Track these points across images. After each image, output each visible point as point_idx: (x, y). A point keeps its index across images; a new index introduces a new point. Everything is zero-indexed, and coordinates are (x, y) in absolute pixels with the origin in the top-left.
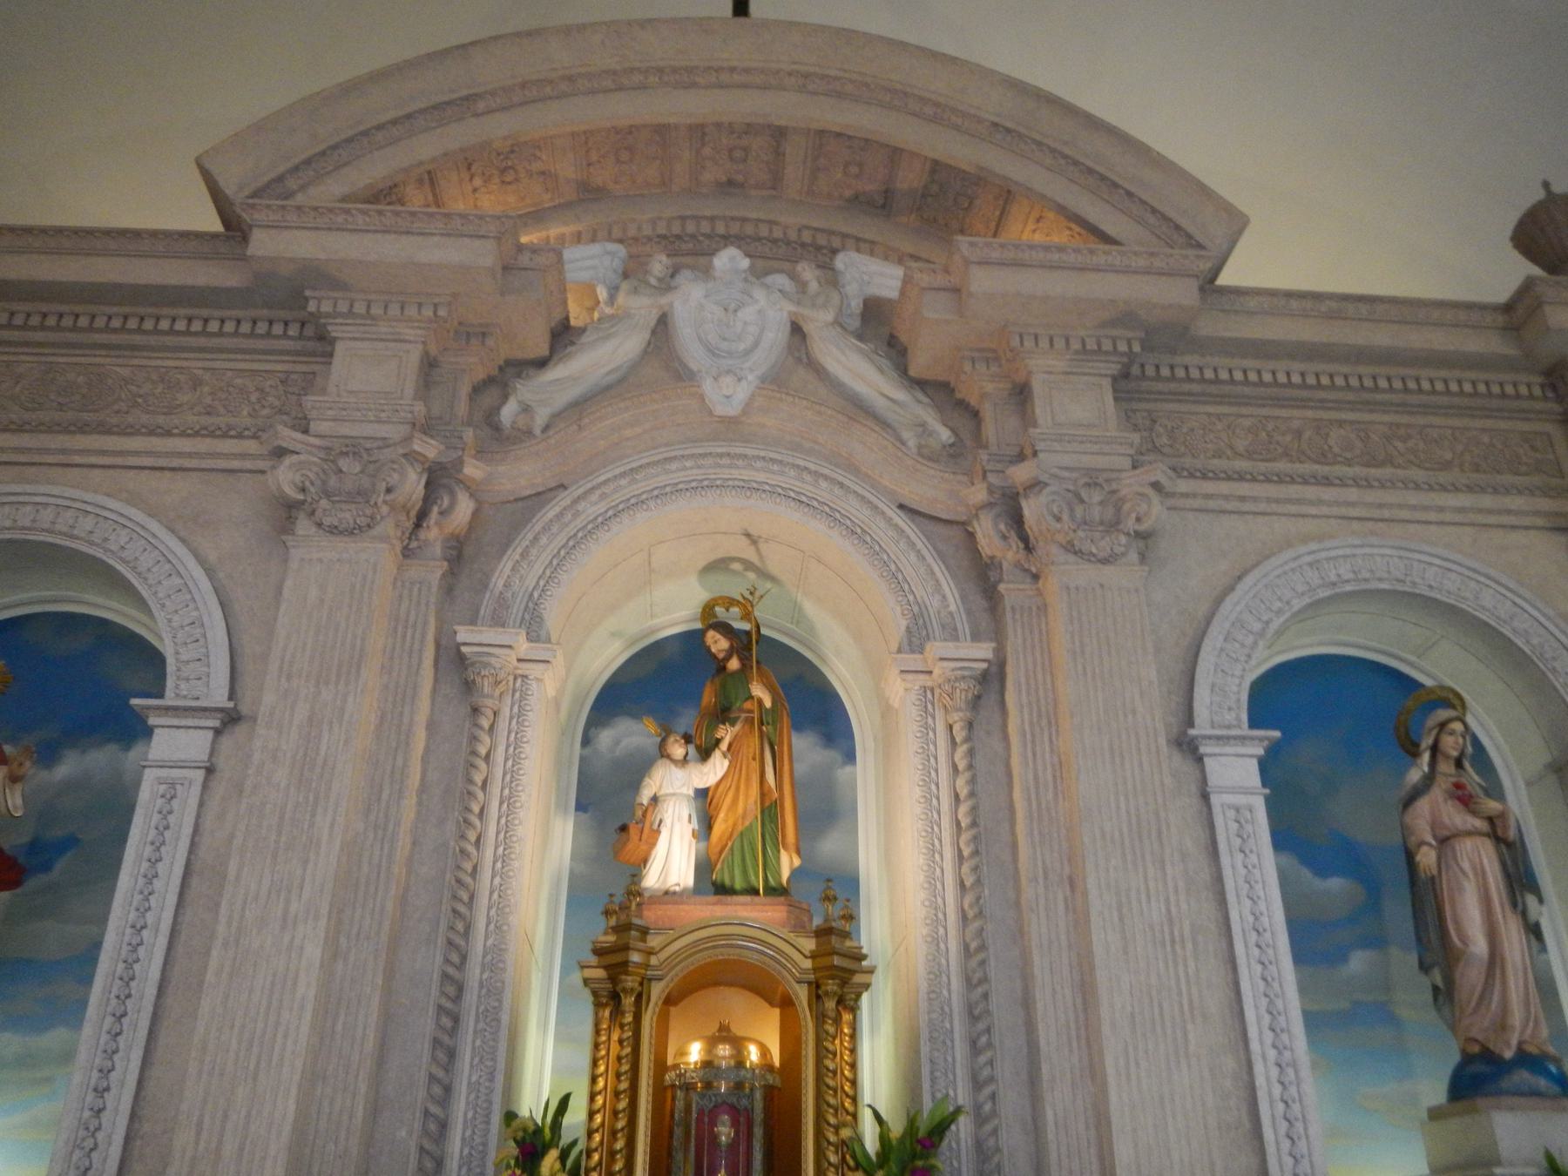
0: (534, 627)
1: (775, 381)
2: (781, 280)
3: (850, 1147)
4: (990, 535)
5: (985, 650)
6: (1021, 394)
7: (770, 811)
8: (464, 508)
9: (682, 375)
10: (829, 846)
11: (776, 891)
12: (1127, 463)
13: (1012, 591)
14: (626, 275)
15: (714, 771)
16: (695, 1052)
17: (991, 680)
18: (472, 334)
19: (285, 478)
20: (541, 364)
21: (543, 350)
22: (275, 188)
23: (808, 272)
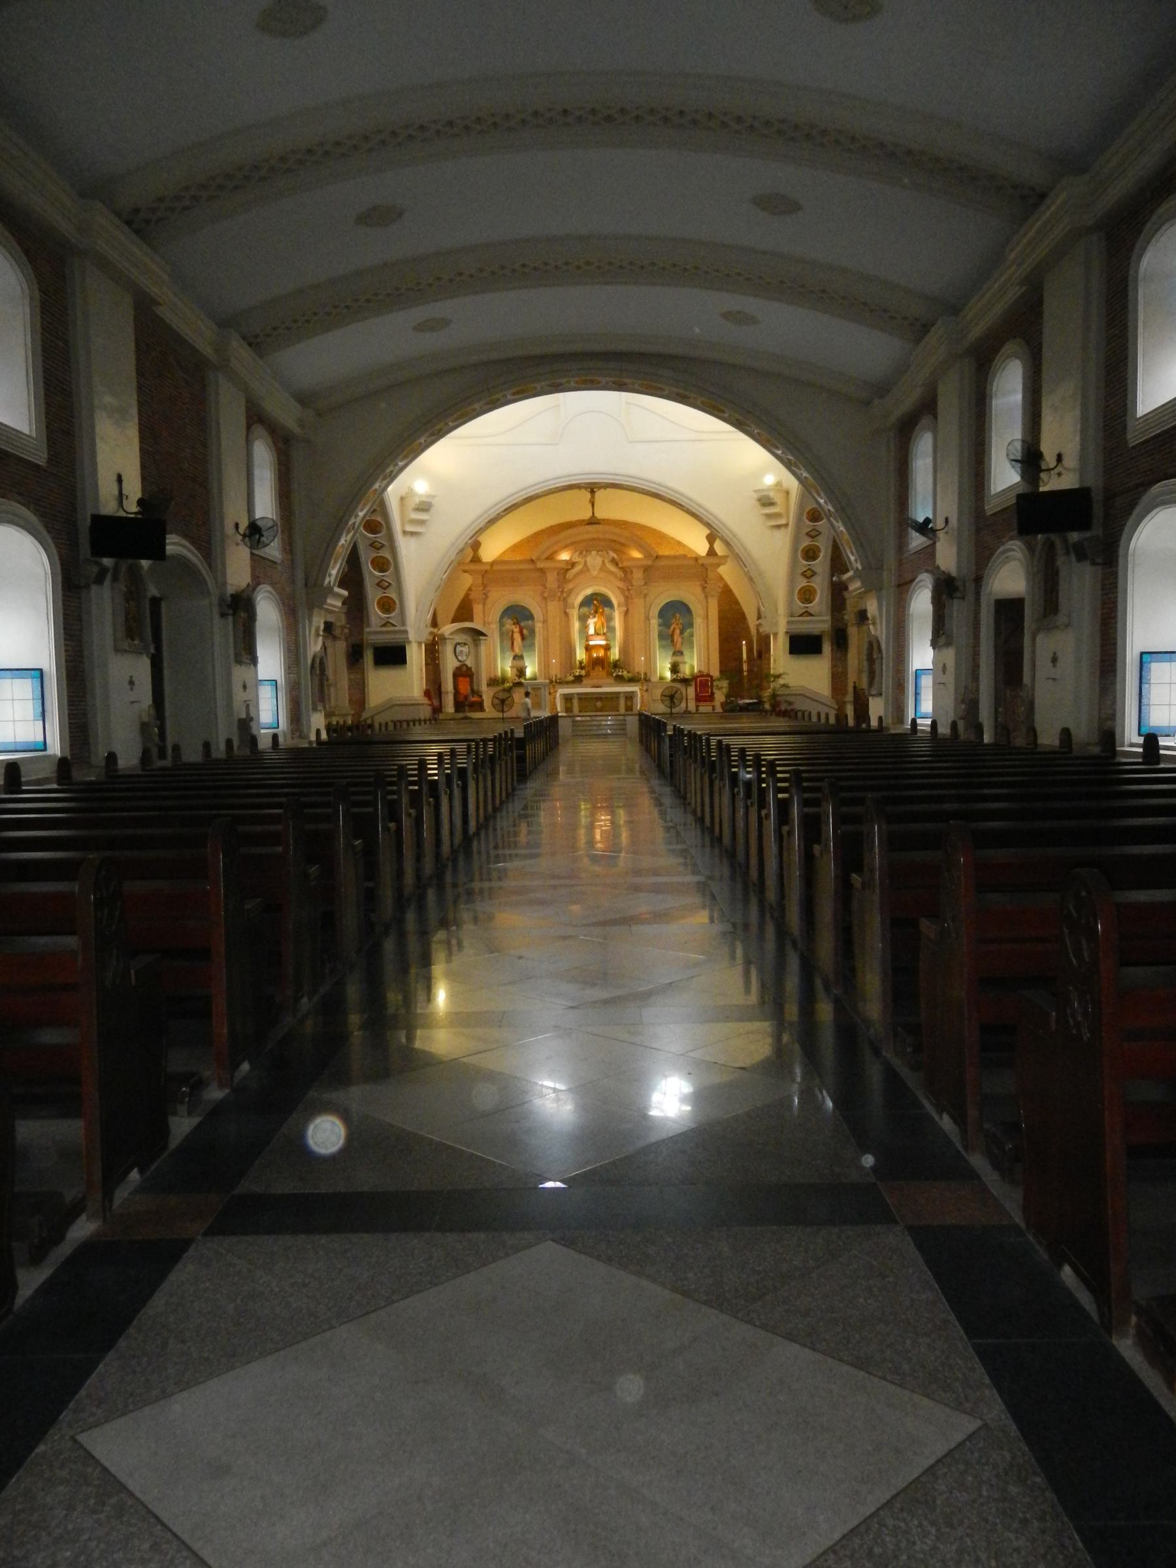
0: (574, 608)
1: (600, 570)
2: (600, 553)
3: (610, 663)
4: (626, 593)
5: (625, 609)
6: (632, 572)
7: (603, 624)
8: (565, 595)
9: (588, 570)
10: (612, 624)
11: (604, 634)
12: (643, 583)
13: (629, 601)
14: (581, 553)
15: (595, 620)
16: (595, 655)
17: (628, 610)
18: (562, 569)
19: (545, 595)
20: (570, 569)
21: (570, 567)
22: (538, 559)
23: (605, 552)
